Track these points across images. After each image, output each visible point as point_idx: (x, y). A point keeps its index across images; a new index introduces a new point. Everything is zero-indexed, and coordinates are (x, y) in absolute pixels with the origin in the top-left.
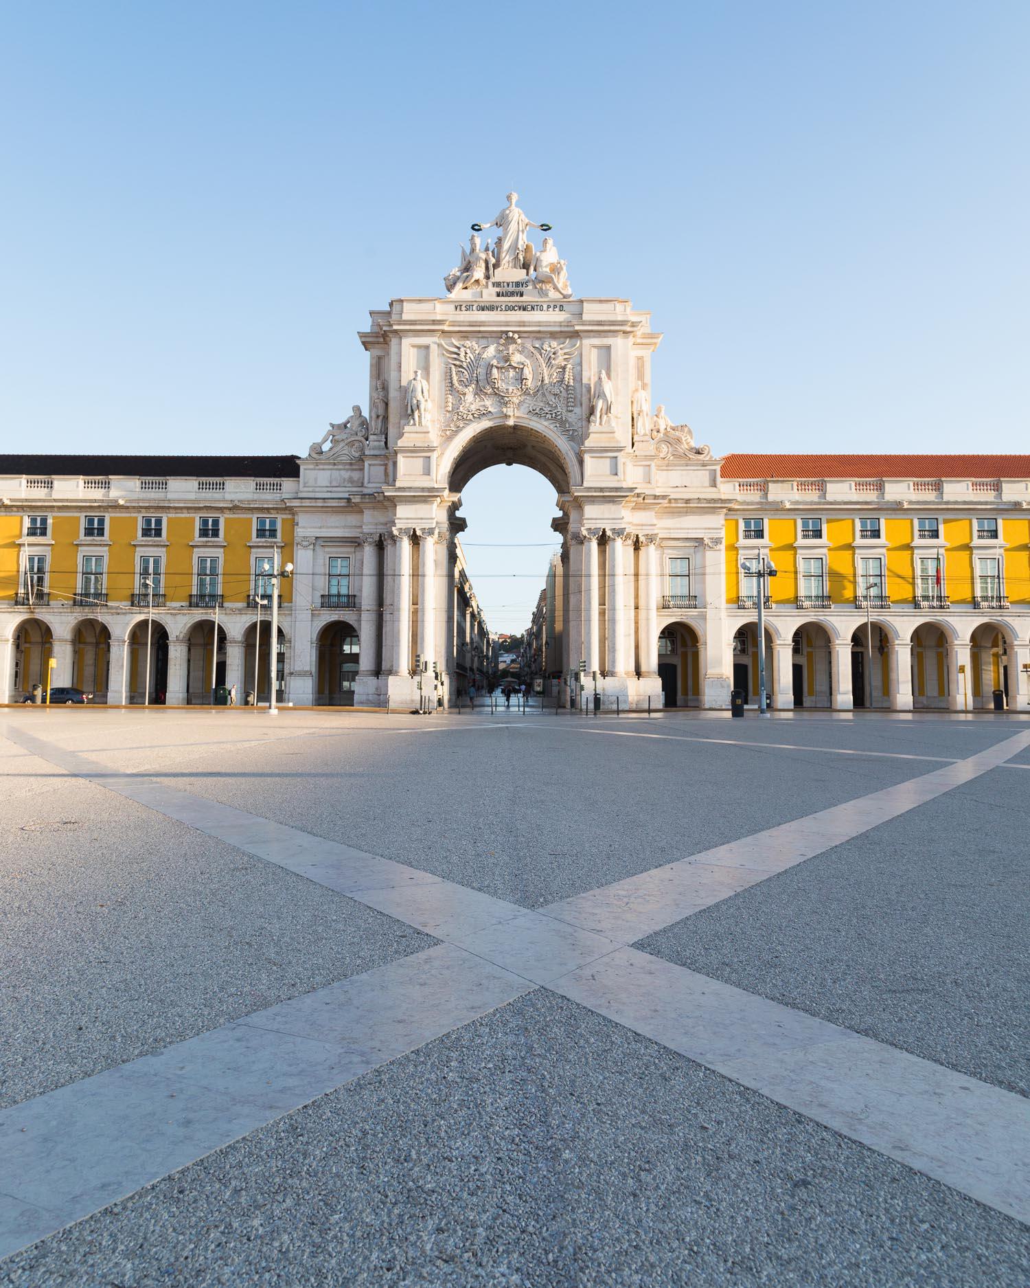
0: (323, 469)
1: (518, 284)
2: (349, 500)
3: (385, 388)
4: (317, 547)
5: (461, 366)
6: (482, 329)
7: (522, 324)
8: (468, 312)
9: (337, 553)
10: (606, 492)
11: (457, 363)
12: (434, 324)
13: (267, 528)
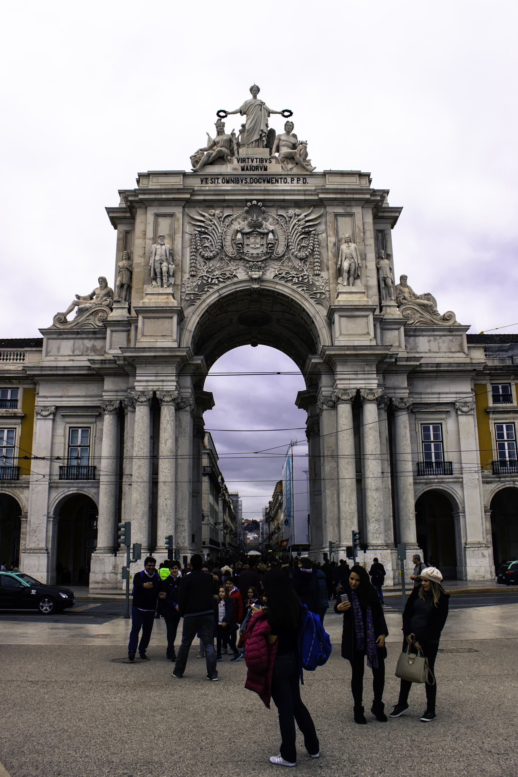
0: (67, 339)
1: (262, 160)
2: (89, 368)
3: (129, 258)
4: (58, 419)
5: (205, 233)
6: (227, 198)
7: (267, 192)
8: (213, 185)
9: (77, 423)
10: (360, 350)
11: (203, 229)
12: (179, 193)
13: (9, 398)
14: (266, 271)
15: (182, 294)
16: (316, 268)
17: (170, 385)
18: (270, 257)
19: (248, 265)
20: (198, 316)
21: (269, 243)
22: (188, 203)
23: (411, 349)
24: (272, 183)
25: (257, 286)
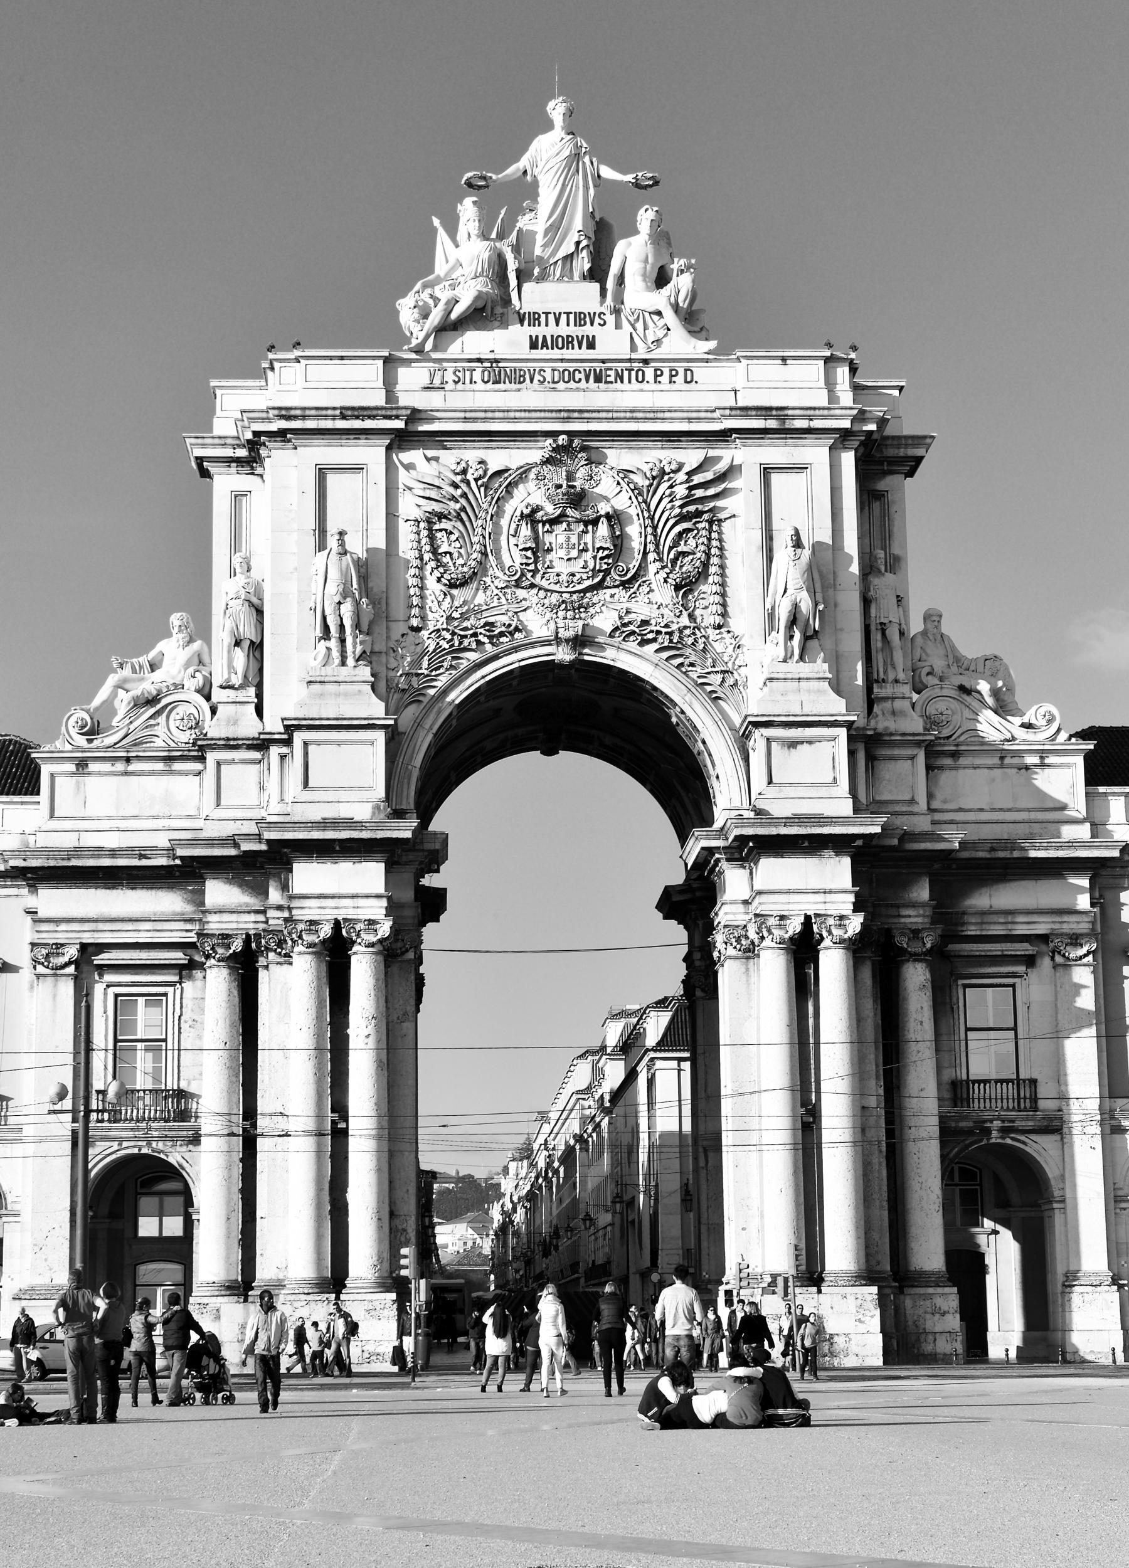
1: (580, 319)
8: (460, 386)
11: (437, 507)
14: (592, 617)
15: (391, 674)
16: (714, 608)
17: (376, 909)
18: (603, 580)
19: (546, 601)
20: (431, 728)
21: (599, 549)
22: (401, 440)
23: (945, 802)
24: (606, 382)
25: (573, 657)
